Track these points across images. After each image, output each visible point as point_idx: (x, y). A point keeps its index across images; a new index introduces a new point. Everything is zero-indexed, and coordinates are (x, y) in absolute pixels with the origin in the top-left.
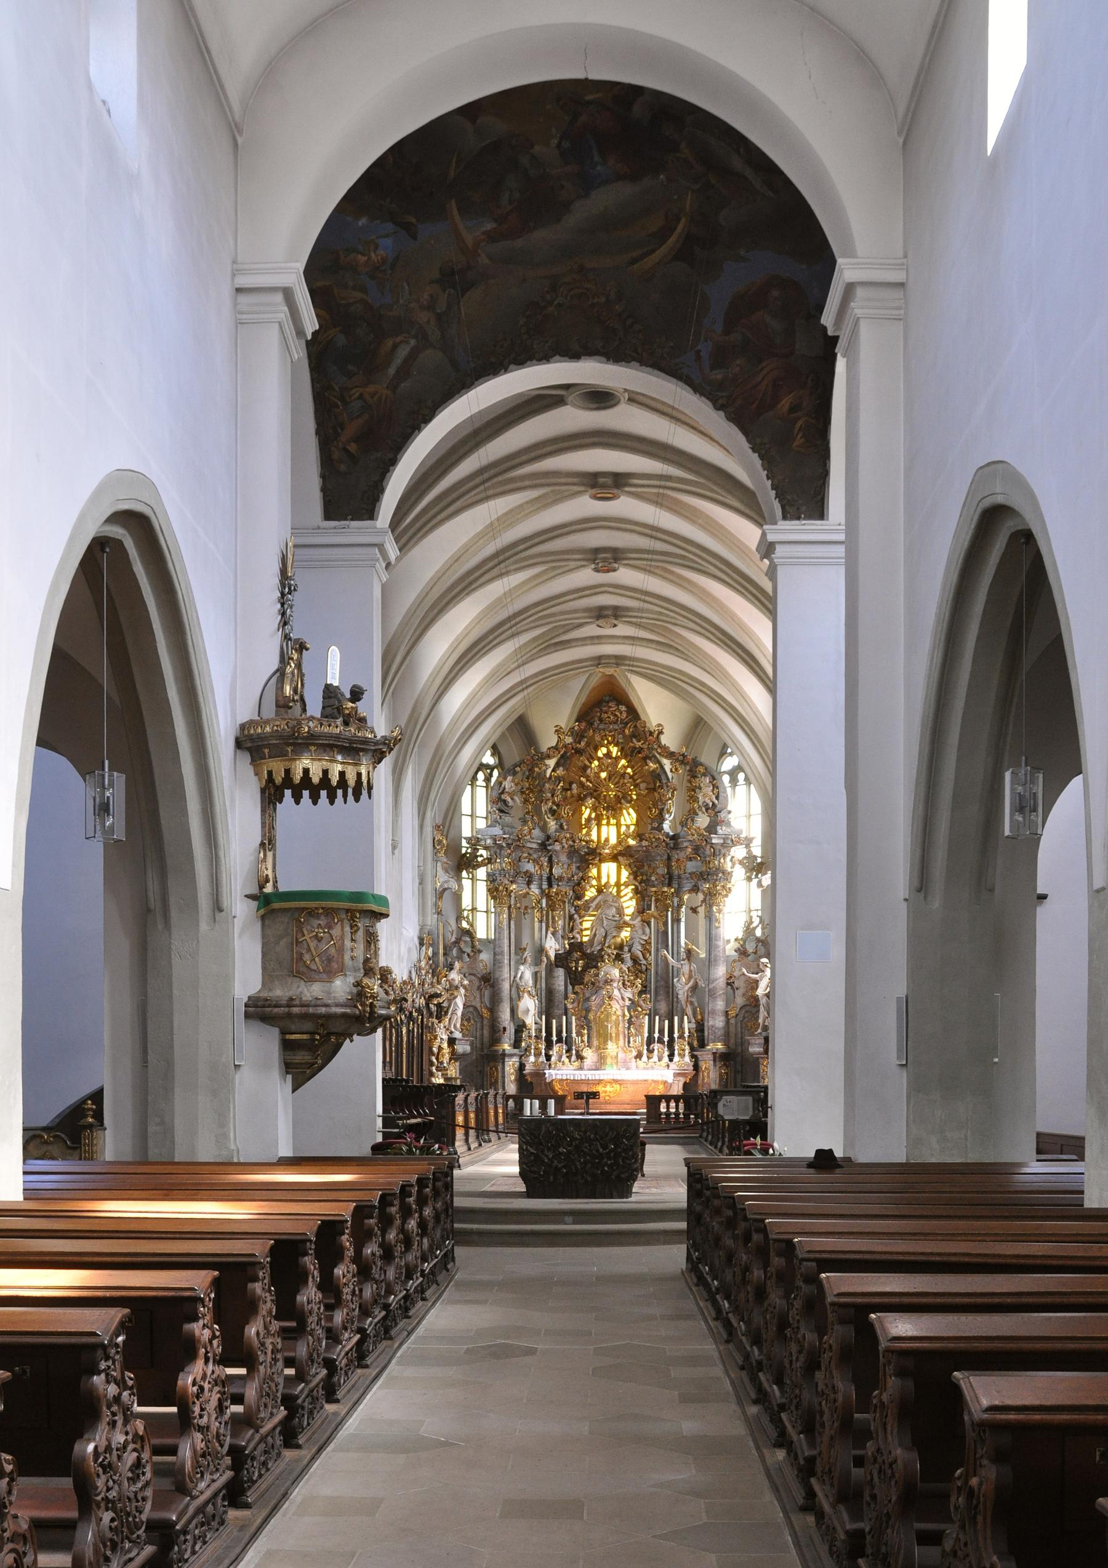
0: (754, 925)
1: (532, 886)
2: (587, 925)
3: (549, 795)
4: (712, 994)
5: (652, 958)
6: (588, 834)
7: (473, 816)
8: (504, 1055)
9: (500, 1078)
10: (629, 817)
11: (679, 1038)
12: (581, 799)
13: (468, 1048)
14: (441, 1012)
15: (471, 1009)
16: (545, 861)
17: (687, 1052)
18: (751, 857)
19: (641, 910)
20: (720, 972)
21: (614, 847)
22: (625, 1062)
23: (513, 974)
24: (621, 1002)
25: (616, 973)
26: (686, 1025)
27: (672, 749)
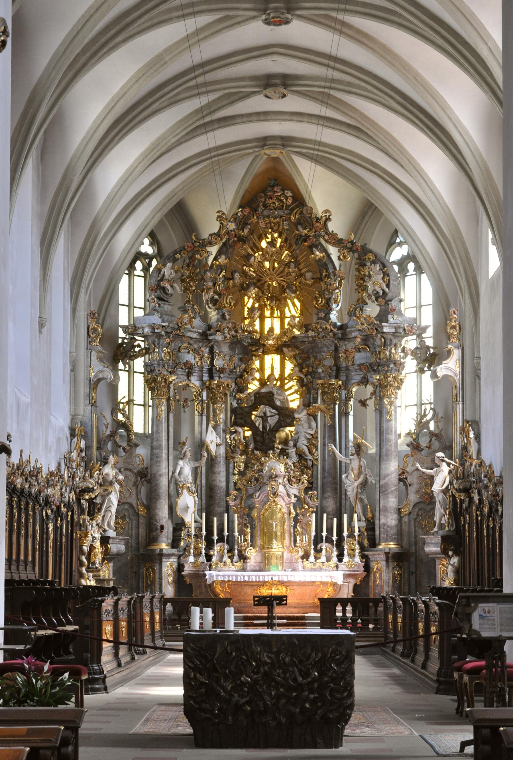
3: (211, 284)
4: (383, 490)
5: (318, 453)
6: (252, 324)
7: (130, 306)
8: (161, 555)
9: (157, 580)
11: (348, 537)
12: (244, 289)
13: (122, 548)
14: (94, 509)
15: (126, 507)
16: (206, 351)
17: (357, 551)
18: (422, 347)
20: (392, 467)
21: (279, 338)
22: (291, 562)
23: (171, 469)
24: (286, 498)
25: (280, 468)
26: (356, 524)
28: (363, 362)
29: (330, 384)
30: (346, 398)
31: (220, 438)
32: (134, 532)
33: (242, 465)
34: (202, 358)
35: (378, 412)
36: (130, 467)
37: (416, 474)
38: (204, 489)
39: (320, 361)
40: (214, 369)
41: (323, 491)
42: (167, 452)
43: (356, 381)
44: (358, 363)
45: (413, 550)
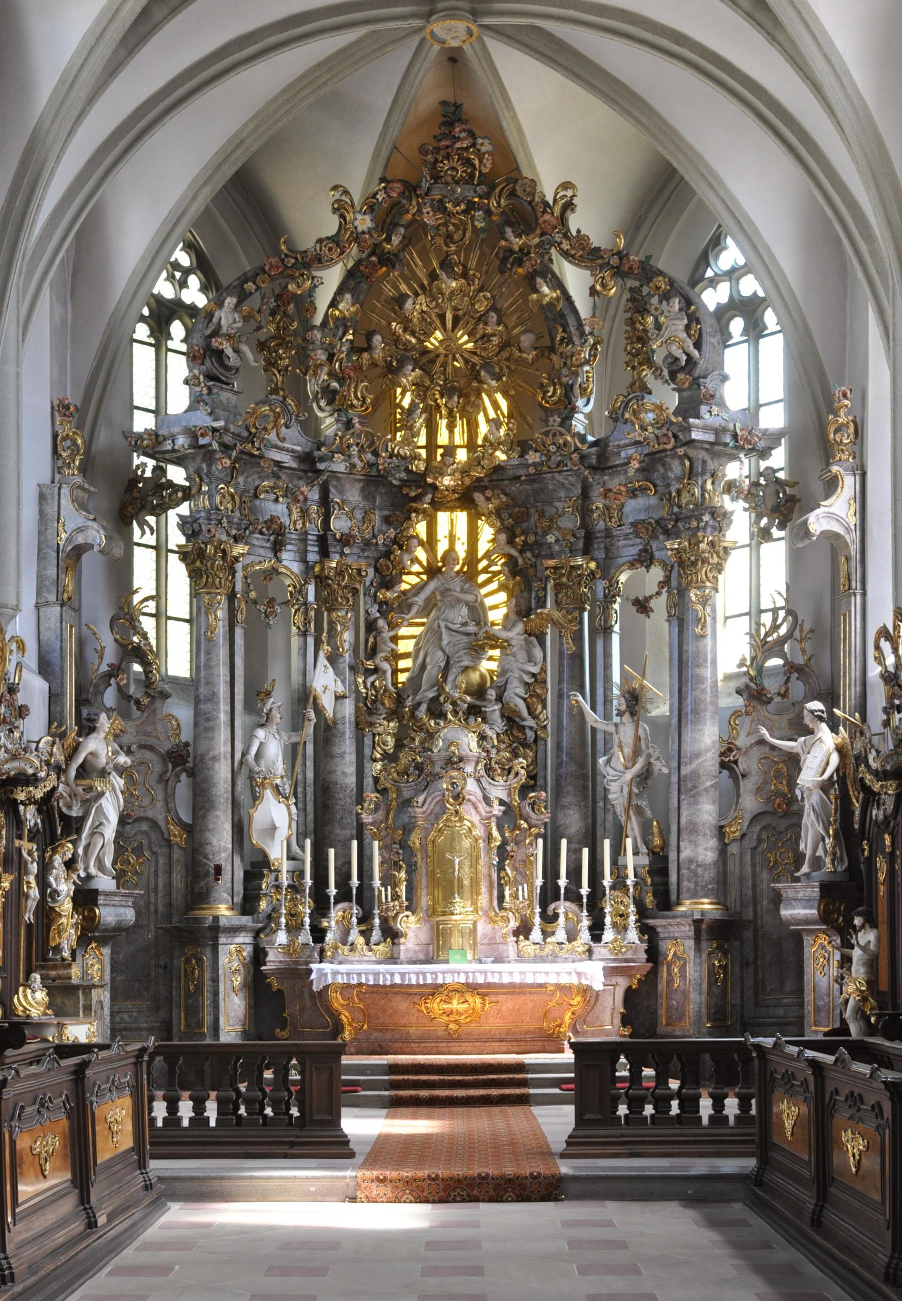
0: (783, 630)
1: (285, 555)
2: (405, 646)
3: (321, 356)
4: (686, 786)
6: (408, 441)
9: (207, 983)
10: (494, 407)
11: (613, 888)
13: (129, 915)
15: (145, 827)
17: (632, 918)
20: (707, 737)
22: (492, 942)
23: (239, 747)
24: (482, 807)
25: (469, 743)
26: (630, 860)
27: (596, 241)
28: (642, 517)
29: (572, 567)
30: (605, 596)
31: (343, 682)
32: (160, 879)
33: (391, 741)
34: (304, 513)
35: (675, 622)
36: (152, 741)
37: (756, 752)
38: (310, 790)
39: (551, 521)
40: (329, 537)
41: (558, 794)
42: (228, 708)
43: (626, 559)
44: (631, 520)
45: (749, 915)
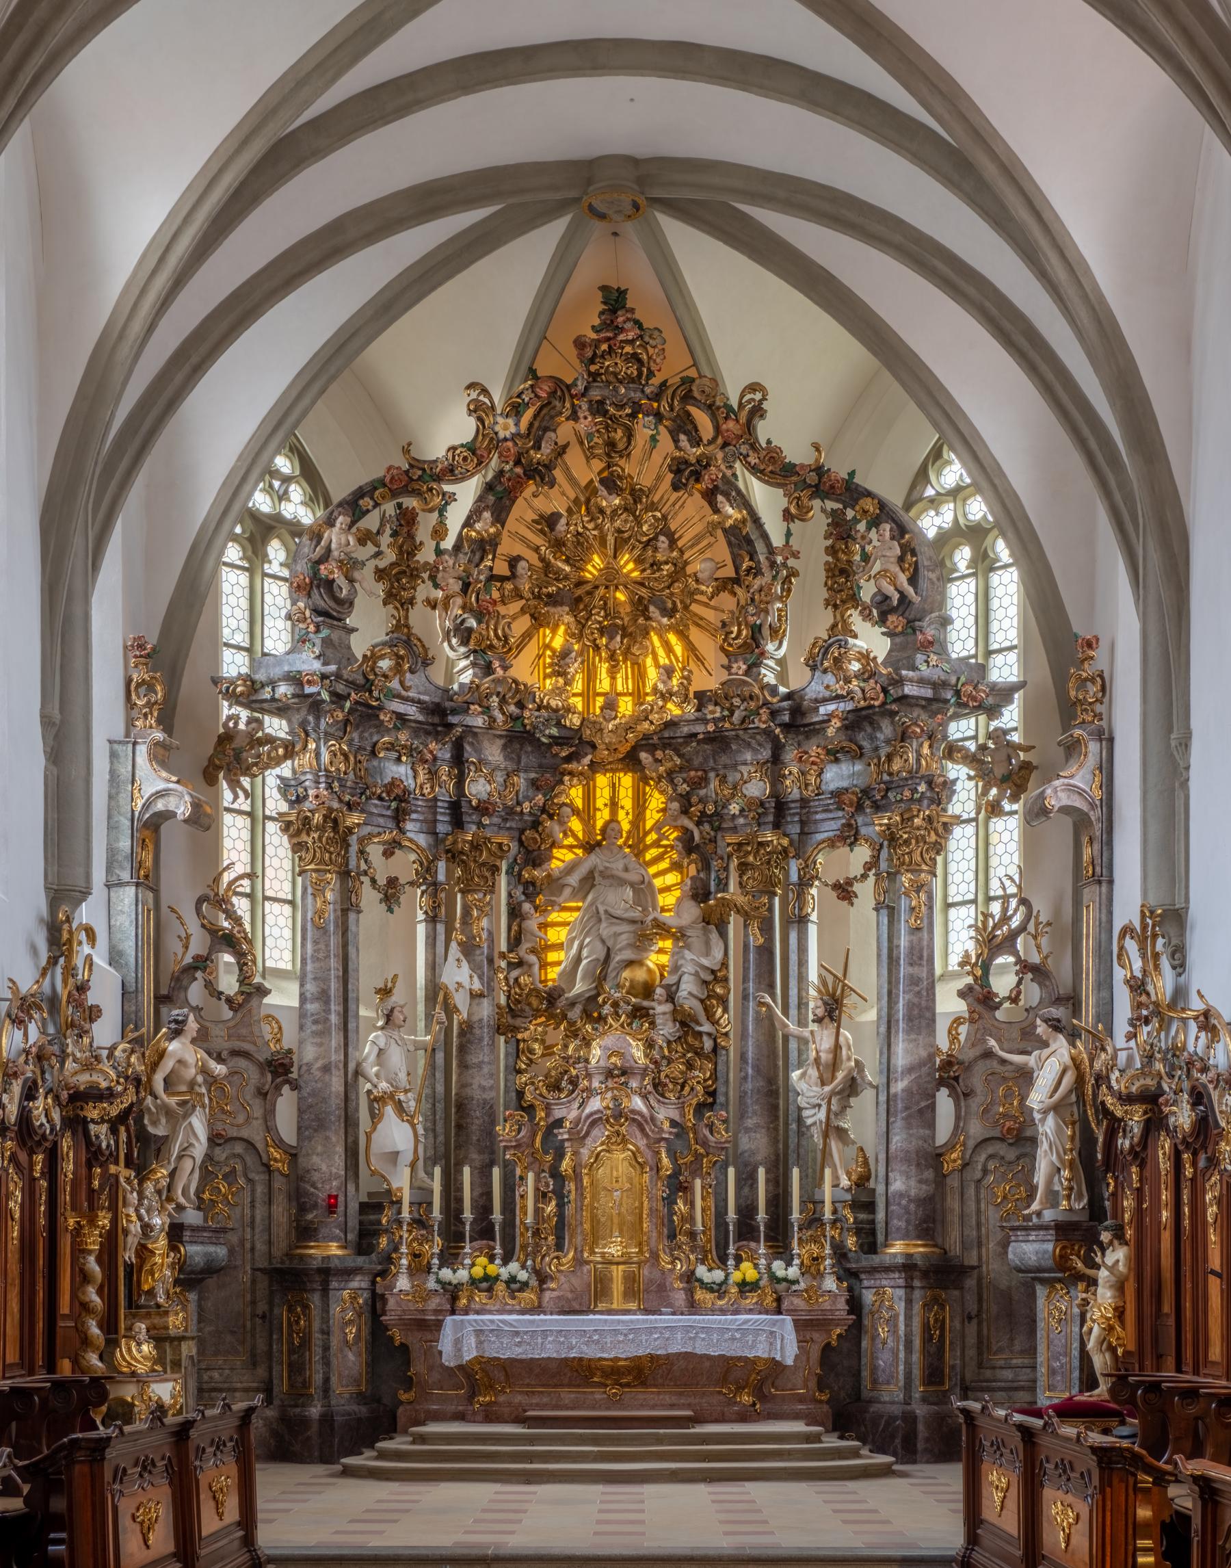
0: (1015, 923)
10: (663, 652)
15: (239, 1148)
19: (700, 894)
